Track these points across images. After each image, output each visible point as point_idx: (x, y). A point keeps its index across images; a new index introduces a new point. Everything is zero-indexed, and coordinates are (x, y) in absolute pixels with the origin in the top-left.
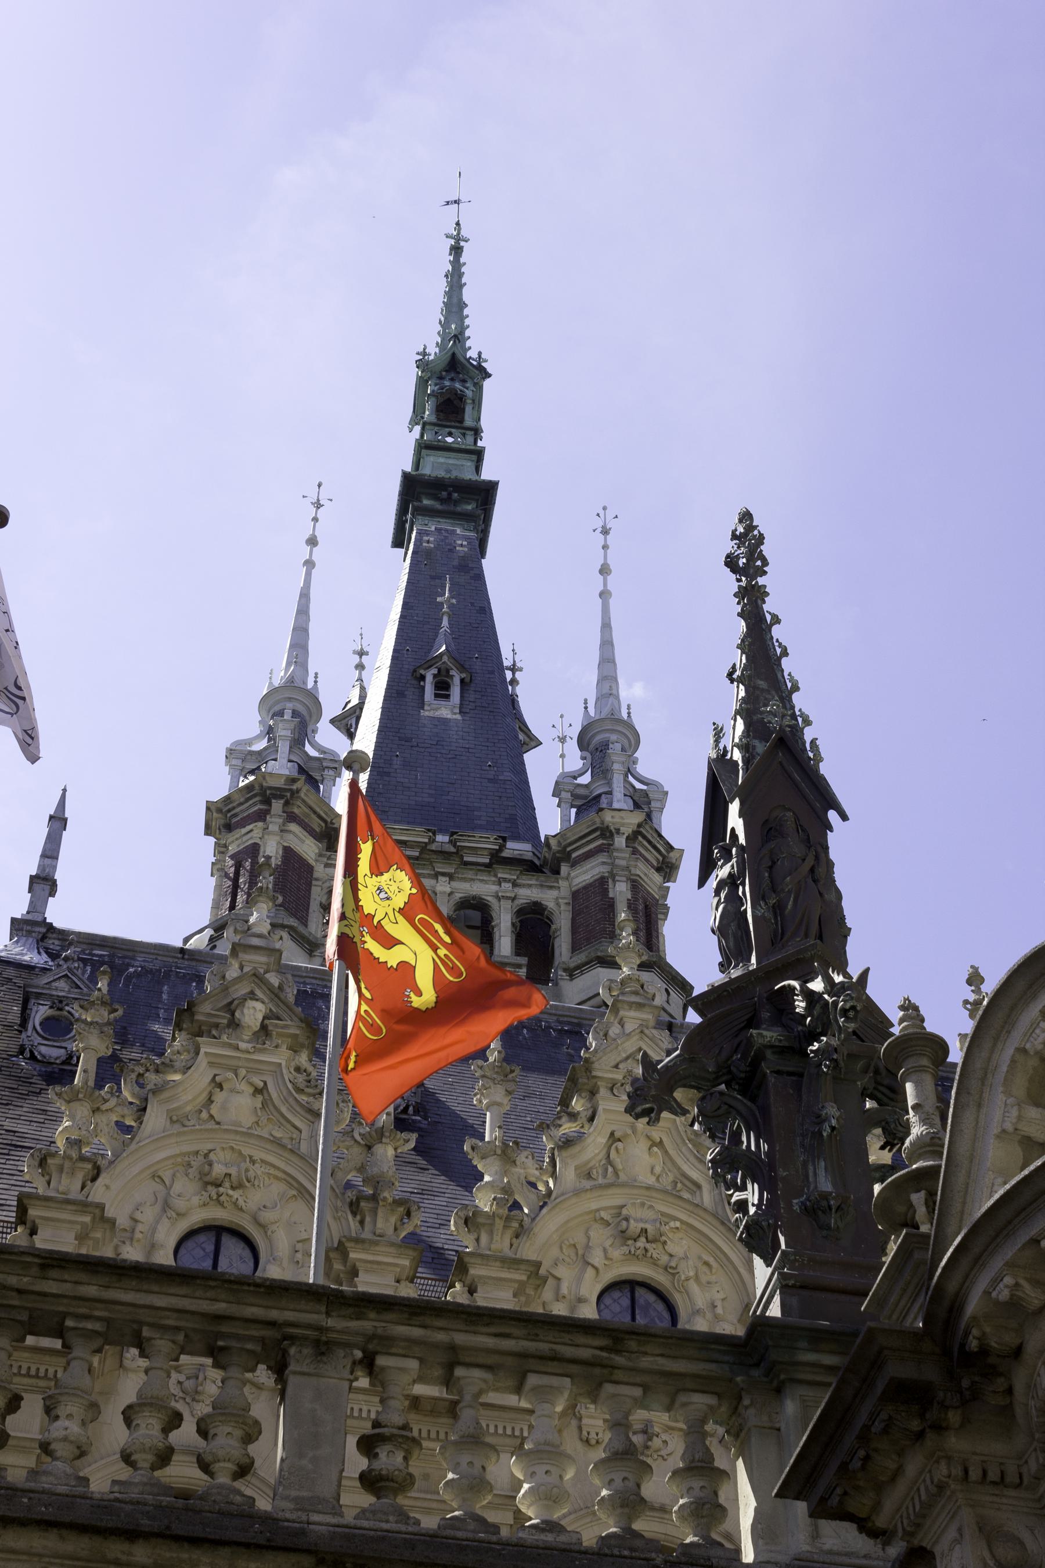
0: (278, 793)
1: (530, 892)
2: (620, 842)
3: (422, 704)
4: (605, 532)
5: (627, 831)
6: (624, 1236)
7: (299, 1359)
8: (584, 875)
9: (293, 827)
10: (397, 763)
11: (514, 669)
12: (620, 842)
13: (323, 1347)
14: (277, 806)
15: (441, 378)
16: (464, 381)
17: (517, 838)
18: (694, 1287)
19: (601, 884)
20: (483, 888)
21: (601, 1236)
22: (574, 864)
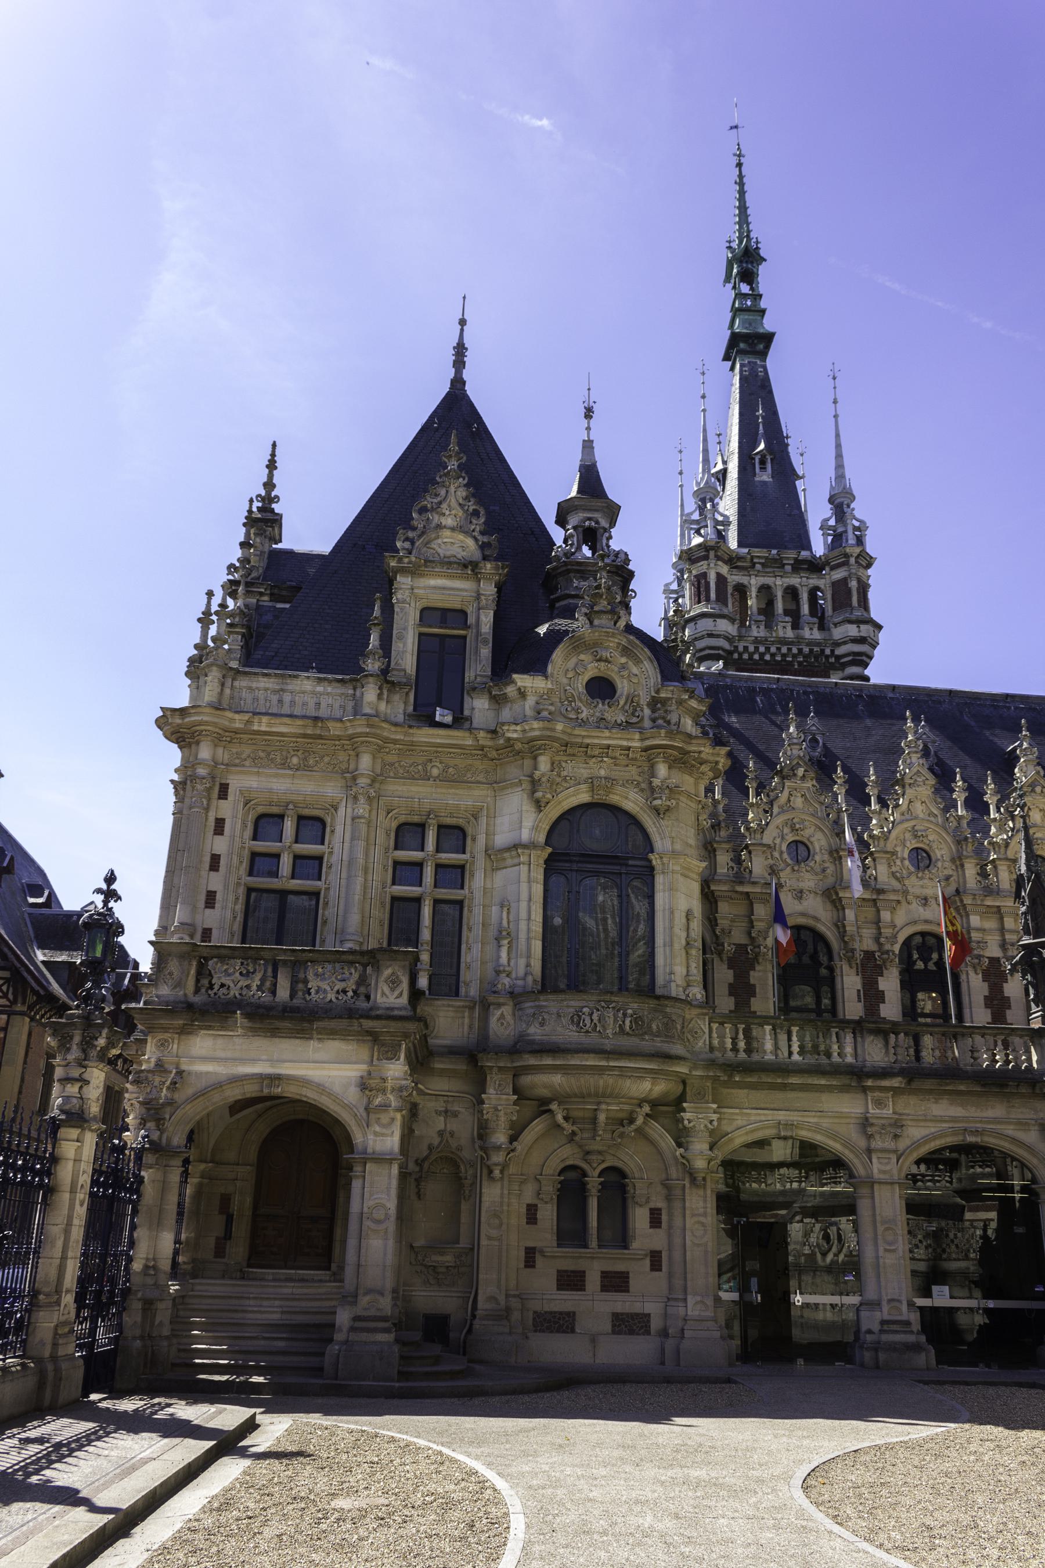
0: (712, 548)
1: (814, 582)
2: (852, 560)
3: (755, 475)
4: (834, 378)
5: (855, 555)
6: (916, 836)
7: (959, 1038)
8: (838, 575)
9: (720, 563)
10: (748, 509)
11: (787, 437)
12: (852, 560)
13: (963, 1035)
14: (712, 554)
15: (741, 262)
16: (752, 263)
17: (803, 549)
18: (937, 851)
19: (844, 581)
20: (794, 581)
21: (908, 835)
22: (832, 569)
